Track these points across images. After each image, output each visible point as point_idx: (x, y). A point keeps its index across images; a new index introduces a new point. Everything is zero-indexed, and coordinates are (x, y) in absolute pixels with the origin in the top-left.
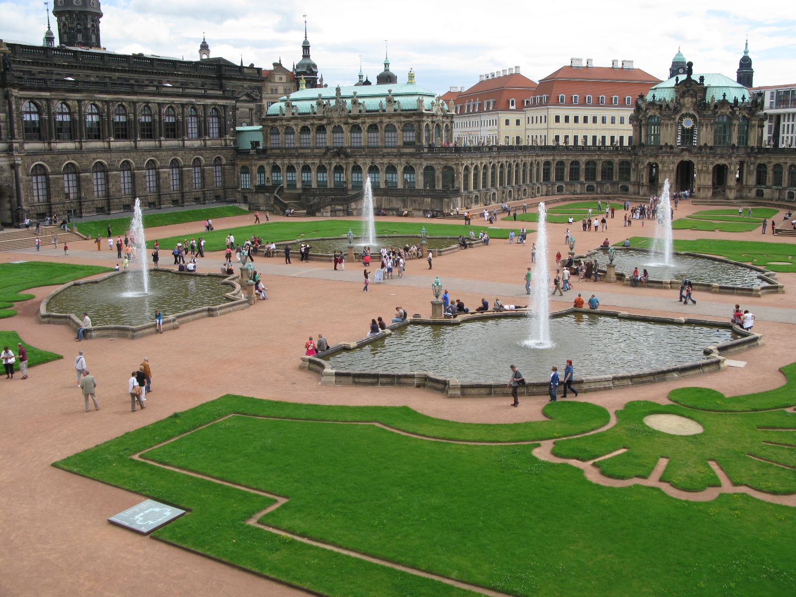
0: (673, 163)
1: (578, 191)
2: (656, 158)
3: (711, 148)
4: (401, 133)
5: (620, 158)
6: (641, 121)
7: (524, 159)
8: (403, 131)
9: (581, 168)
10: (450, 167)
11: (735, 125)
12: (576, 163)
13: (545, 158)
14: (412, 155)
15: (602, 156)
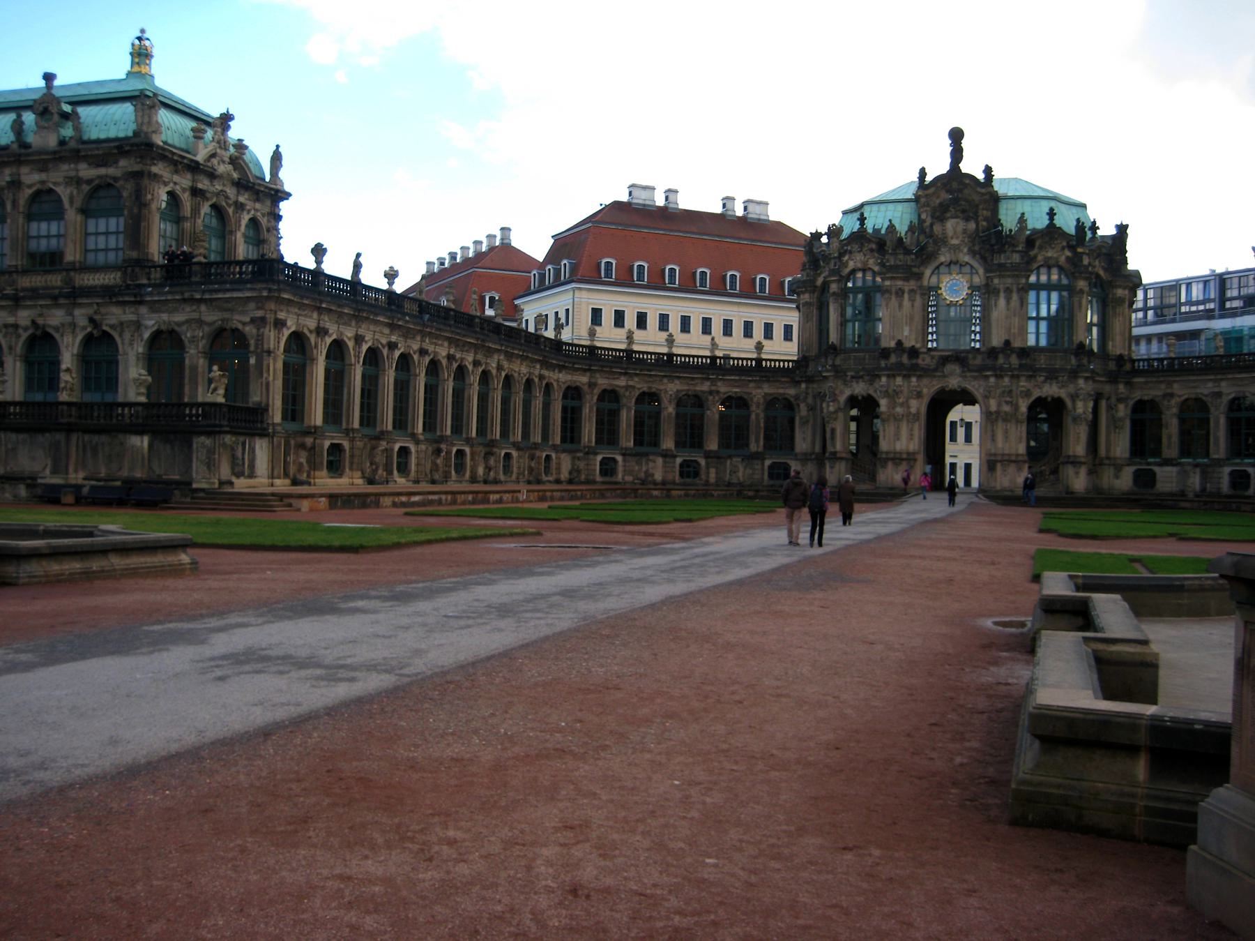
0: (919, 395)
1: (658, 476)
2: (871, 383)
3: (1025, 352)
4: (79, 218)
5: (768, 389)
6: (826, 285)
7: (505, 364)
8: (85, 212)
9: (664, 414)
10: (235, 331)
11: (1082, 291)
12: (649, 397)
13: (569, 377)
14: (109, 294)
15: (719, 384)
